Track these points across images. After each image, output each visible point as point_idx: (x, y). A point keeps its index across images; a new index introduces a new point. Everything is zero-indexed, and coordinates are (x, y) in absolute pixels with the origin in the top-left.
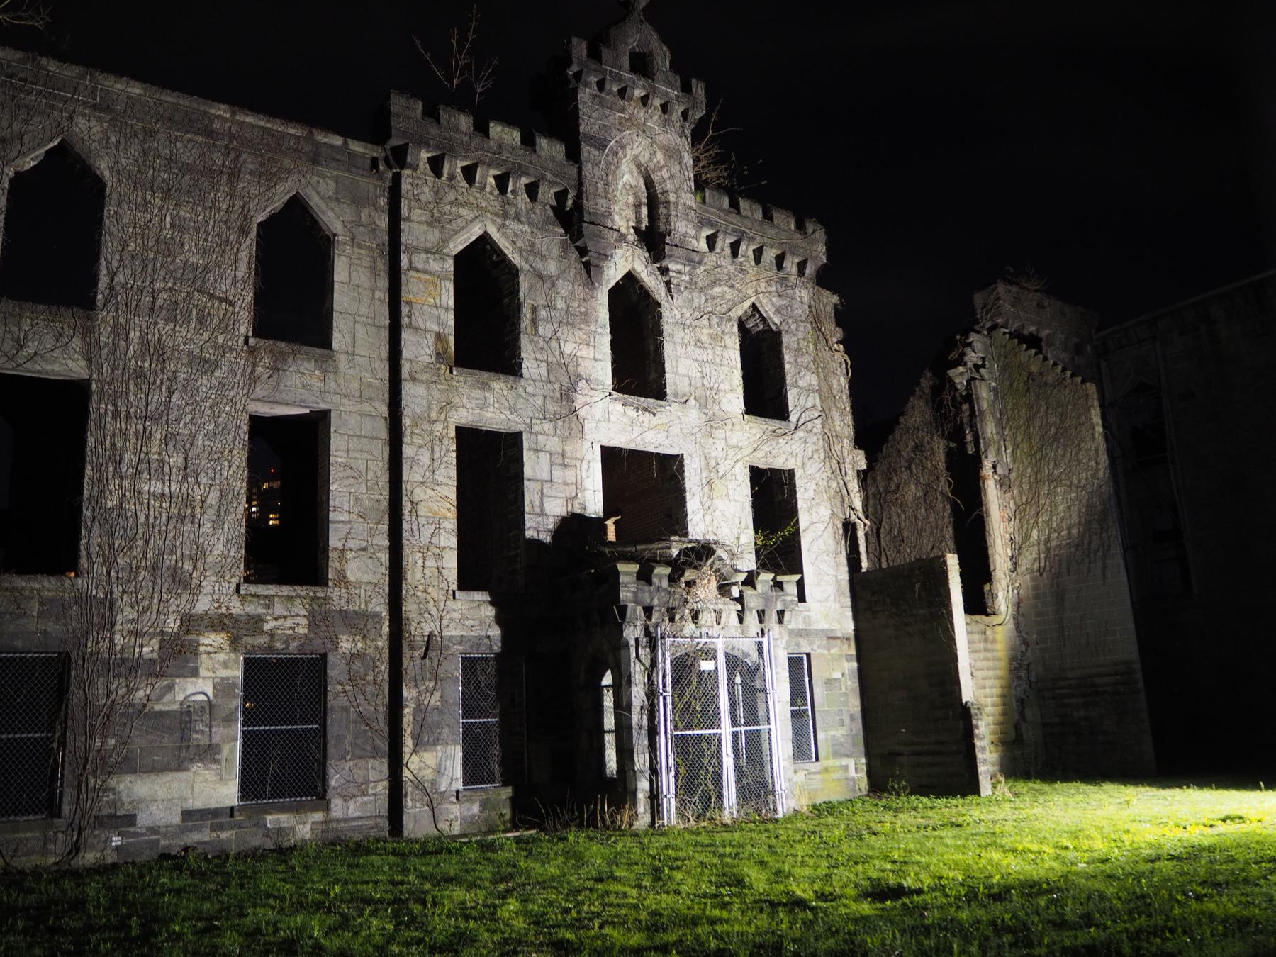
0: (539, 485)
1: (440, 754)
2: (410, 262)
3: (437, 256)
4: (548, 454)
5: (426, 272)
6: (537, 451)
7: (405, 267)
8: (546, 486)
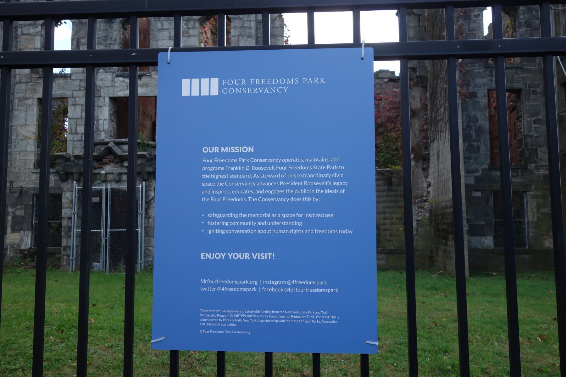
0: (75, 120)
1: (22, 234)
2: (22, 31)
3: (34, 26)
4: (80, 106)
5: (28, 34)
6: (74, 105)
7: (20, 35)
8: (79, 120)
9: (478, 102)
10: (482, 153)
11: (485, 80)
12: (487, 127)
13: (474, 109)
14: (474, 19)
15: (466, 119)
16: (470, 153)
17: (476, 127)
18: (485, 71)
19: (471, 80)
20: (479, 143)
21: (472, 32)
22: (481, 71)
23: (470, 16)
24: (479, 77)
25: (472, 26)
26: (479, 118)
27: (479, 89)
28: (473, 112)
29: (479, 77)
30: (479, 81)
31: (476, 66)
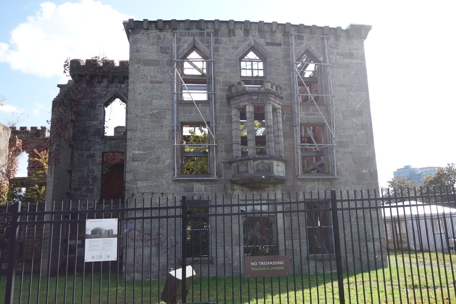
9: (95, 160)
10: (95, 193)
11: (101, 146)
12: (100, 176)
13: (93, 165)
14: (98, 108)
15: (87, 171)
16: (87, 193)
17: (93, 176)
18: (101, 140)
19: (92, 146)
20: (94, 187)
21: (96, 116)
22: (99, 140)
23: (95, 106)
24: (97, 144)
25: (96, 112)
26: (95, 170)
27: (97, 152)
28: (92, 167)
29: (97, 144)
30: (97, 147)
31: (96, 137)
